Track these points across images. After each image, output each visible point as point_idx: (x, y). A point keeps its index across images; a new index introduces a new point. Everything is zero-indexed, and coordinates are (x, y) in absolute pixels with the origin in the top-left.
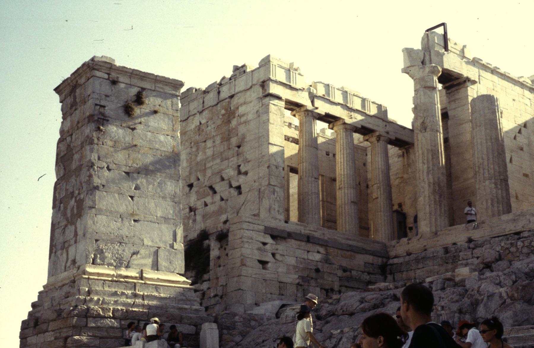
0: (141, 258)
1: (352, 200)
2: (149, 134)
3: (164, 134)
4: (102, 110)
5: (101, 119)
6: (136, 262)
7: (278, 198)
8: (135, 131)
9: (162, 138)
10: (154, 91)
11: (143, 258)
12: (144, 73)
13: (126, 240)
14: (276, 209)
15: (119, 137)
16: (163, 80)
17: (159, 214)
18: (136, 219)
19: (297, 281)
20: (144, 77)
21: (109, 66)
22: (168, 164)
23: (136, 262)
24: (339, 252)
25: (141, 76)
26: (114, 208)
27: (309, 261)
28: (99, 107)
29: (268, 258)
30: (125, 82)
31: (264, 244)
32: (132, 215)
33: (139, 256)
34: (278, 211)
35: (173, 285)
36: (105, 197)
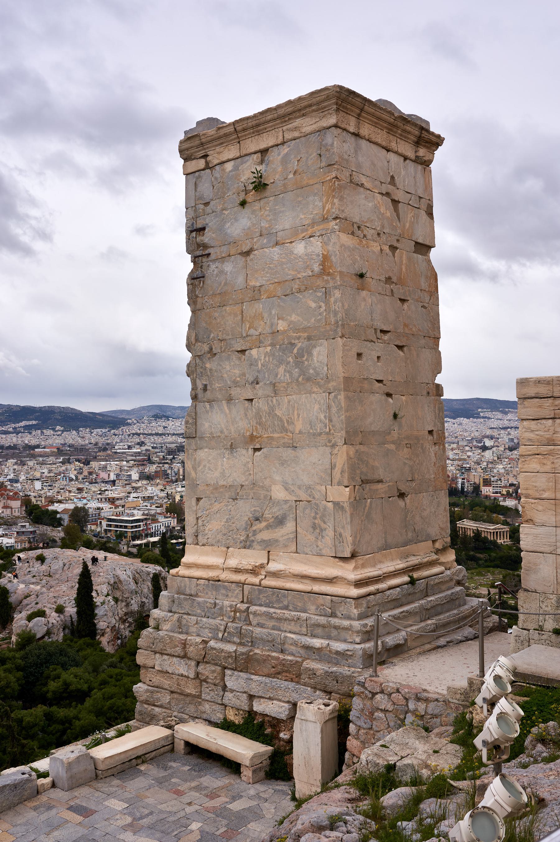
0: (267, 527)
2: (276, 249)
3: (303, 239)
4: (199, 239)
5: (198, 256)
6: (259, 537)
8: (252, 256)
9: (300, 248)
10: (283, 143)
12: (255, 116)
15: (226, 284)
18: (258, 446)
20: (258, 125)
21: (197, 142)
22: (313, 305)
23: (259, 537)
25: (253, 127)
26: (222, 432)
28: (194, 234)
30: (231, 157)
32: (252, 438)
33: (264, 524)
35: (317, 588)
36: (207, 412)
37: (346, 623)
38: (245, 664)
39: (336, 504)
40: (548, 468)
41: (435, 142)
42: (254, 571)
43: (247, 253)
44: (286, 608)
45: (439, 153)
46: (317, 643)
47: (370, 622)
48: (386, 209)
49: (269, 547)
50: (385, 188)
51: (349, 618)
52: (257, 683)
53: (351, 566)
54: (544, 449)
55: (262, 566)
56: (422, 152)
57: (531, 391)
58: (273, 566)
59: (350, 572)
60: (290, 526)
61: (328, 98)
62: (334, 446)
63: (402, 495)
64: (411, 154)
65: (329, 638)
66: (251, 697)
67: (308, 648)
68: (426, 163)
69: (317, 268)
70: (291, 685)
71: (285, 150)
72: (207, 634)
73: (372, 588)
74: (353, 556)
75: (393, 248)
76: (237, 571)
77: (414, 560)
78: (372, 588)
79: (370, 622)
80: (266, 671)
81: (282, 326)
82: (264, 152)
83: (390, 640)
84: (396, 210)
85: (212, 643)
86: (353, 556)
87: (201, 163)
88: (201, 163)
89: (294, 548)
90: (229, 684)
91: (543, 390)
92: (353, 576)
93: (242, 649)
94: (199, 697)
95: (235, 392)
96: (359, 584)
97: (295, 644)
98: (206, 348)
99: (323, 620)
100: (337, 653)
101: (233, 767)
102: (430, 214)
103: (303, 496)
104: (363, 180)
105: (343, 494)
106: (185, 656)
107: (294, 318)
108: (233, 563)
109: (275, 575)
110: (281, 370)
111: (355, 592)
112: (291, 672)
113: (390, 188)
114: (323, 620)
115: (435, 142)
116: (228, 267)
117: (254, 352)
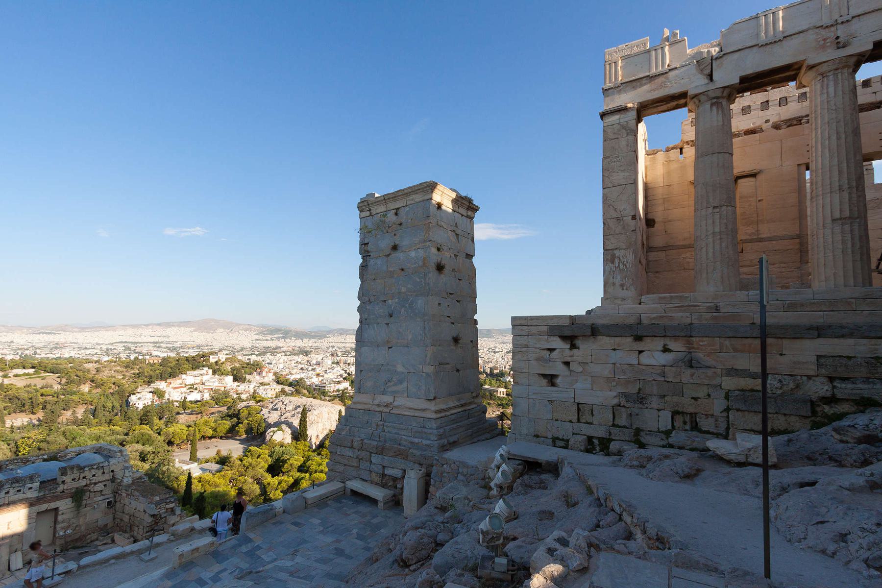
1: (837, 215)
6: (390, 389)
7: (621, 266)
9: (413, 254)
11: (395, 385)
13: (382, 368)
14: (617, 284)
16: (410, 190)
17: (410, 337)
19: (616, 401)
23: (390, 389)
24: (727, 342)
27: (644, 367)
29: (558, 369)
31: (551, 350)
32: (388, 342)
34: (622, 286)
37: (430, 431)
38: (381, 451)
39: (428, 375)
40: (525, 358)
41: (475, 209)
42: (387, 406)
43: (388, 256)
44: (401, 424)
45: (477, 214)
46: (416, 440)
47: (442, 431)
48: (453, 238)
49: (394, 394)
50: (454, 228)
51: (431, 428)
52: (387, 460)
53: (433, 403)
54: (524, 349)
55: (391, 404)
56: (470, 213)
57: (518, 322)
58: (396, 404)
59: (432, 406)
60: (405, 384)
61: (428, 186)
62: (427, 346)
63: (458, 371)
64: (465, 214)
65: (422, 438)
66: (384, 467)
67: (412, 443)
68: (472, 218)
69: (421, 263)
70: (403, 461)
71: (407, 209)
72: (363, 436)
73: (443, 414)
74: (435, 399)
75: (456, 256)
76: (379, 406)
77: (463, 402)
78: (443, 414)
79: (442, 431)
80: (391, 454)
81: (403, 290)
82: (397, 209)
83: (451, 440)
84: (458, 238)
85: (366, 441)
86: (435, 399)
87: (368, 213)
88: (368, 213)
89: (406, 395)
90: (373, 461)
91: (523, 322)
92: (433, 409)
93: (380, 444)
94: (358, 467)
95: (379, 320)
96: (436, 412)
97: (406, 441)
98: (367, 299)
99: (420, 429)
100: (426, 445)
101: (374, 501)
102: (473, 241)
103: (412, 370)
104: (443, 224)
105: (429, 369)
106: (352, 447)
107: (409, 286)
108: (376, 402)
109: (397, 407)
110: (403, 310)
111: (434, 416)
112: (403, 455)
113: (455, 229)
114: (420, 429)
115: (475, 209)
116: (379, 262)
117: (390, 301)
